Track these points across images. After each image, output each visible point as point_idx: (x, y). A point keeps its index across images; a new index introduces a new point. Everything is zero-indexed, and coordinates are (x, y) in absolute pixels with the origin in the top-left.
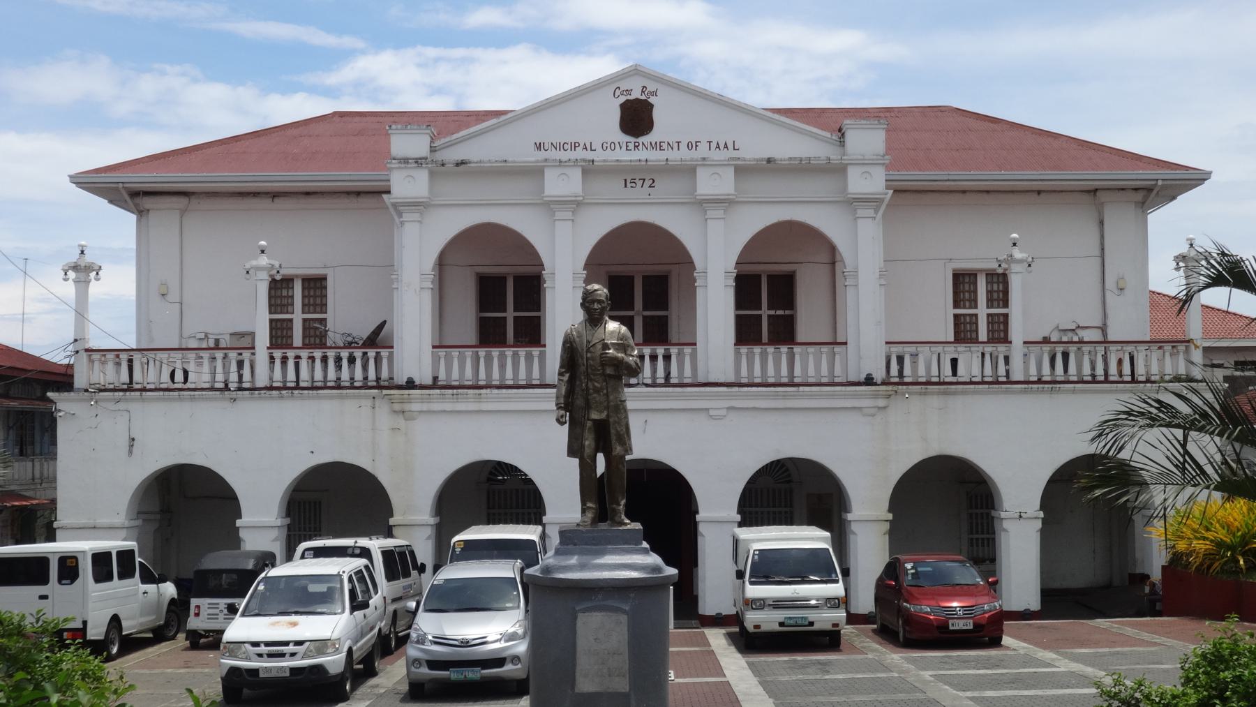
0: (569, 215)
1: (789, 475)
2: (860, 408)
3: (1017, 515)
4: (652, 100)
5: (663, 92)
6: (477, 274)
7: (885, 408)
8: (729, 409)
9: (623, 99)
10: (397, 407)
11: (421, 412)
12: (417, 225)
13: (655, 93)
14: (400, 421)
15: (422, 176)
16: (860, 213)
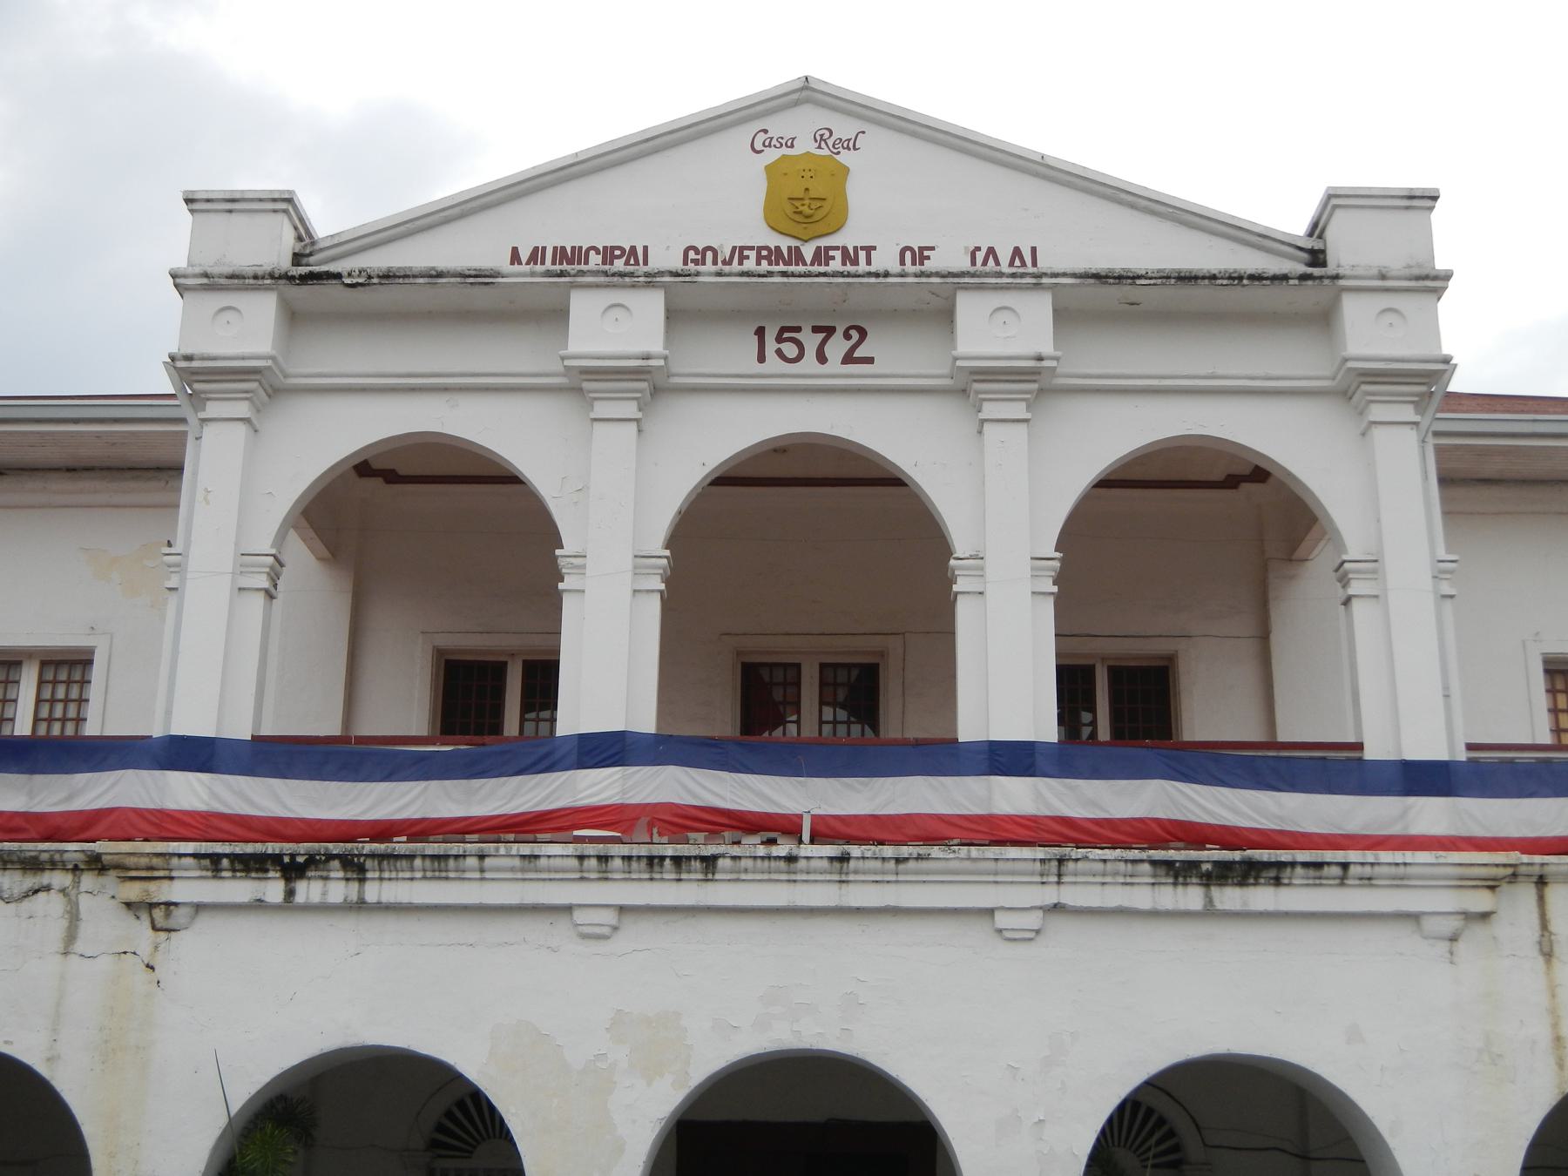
0: (630, 409)
1: (1176, 1148)
2: (1414, 917)
4: (845, 158)
5: (876, 141)
6: (439, 653)
7: (1485, 916)
8: (1057, 908)
9: (772, 155)
10: (133, 891)
11: (199, 908)
12: (241, 429)
13: (851, 145)
14: (140, 933)
15: (263, 309)
16: (1378, 412)
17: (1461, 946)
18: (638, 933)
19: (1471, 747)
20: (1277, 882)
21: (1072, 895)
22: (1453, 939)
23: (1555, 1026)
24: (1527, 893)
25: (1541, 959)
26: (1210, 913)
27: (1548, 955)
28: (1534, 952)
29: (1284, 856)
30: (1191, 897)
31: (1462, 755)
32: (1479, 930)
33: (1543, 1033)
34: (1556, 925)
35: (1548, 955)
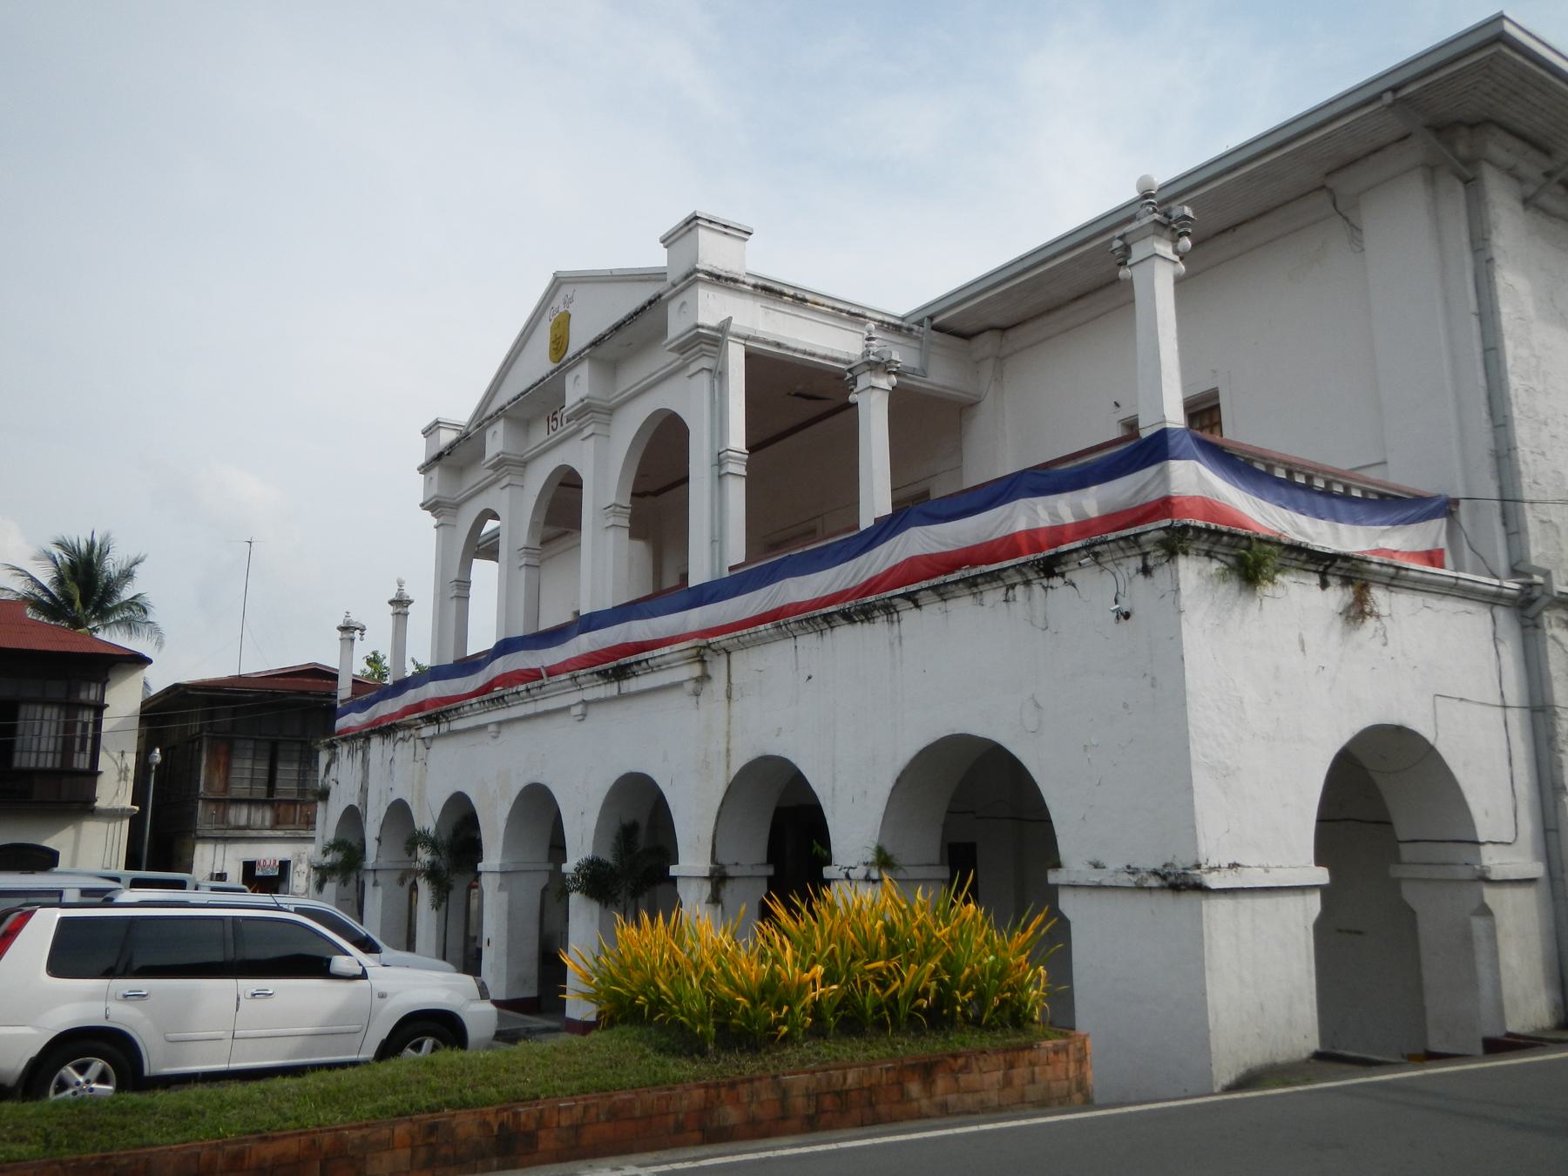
3: (843, 876)
18: (508, 734)
19: (731, 569)
20: (635, 675)
21: (589, 694)
22: (697, 695)
24: (724, 658)
26: (621, 697)
27: (729, 697)
28: (723, 697)
29: (633, 659)
30: (611, 689)
31: (726, 574)
32: (707, 687)
33: (723, 747)
34: (733, 680)
35: (729, 697)
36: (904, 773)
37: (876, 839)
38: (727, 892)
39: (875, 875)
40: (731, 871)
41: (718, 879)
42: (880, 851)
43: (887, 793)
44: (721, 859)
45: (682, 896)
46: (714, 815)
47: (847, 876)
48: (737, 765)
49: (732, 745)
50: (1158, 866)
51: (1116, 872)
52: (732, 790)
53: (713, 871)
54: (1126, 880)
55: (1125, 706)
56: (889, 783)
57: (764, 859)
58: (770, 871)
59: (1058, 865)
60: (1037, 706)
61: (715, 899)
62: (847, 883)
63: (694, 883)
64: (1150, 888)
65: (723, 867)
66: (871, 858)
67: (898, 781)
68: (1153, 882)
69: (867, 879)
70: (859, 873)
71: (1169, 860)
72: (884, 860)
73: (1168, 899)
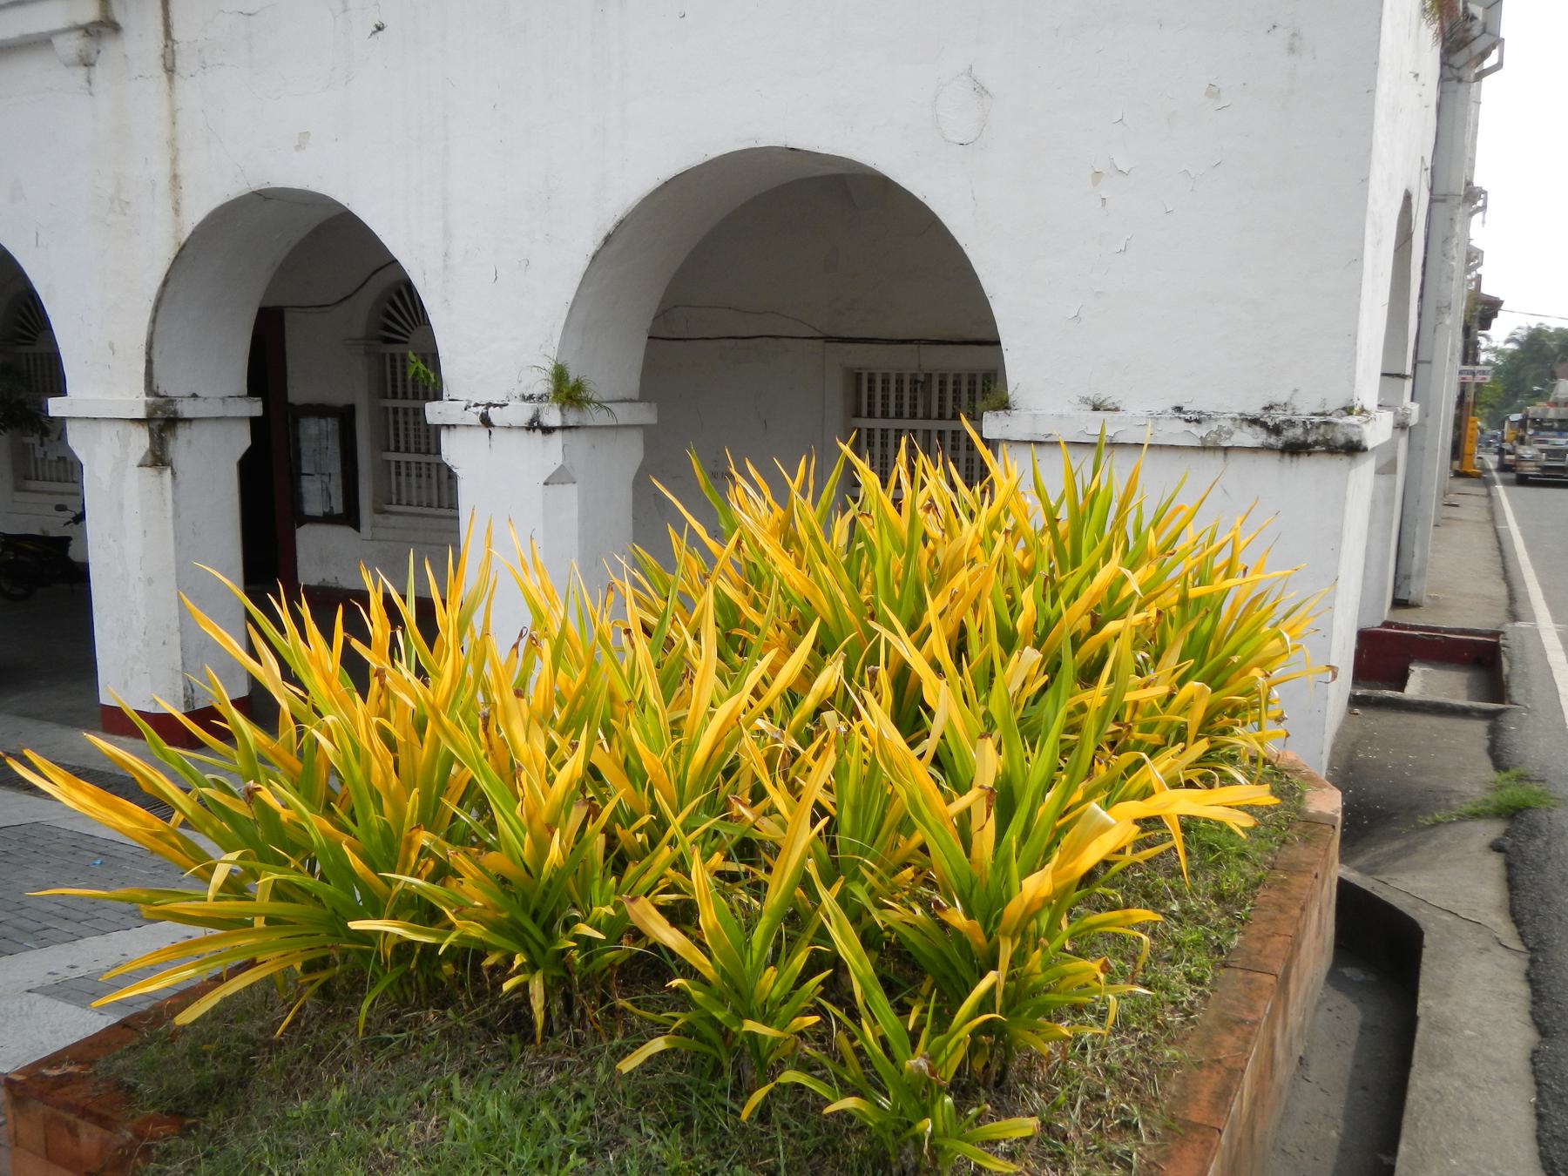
3: (476, 420)
17: (98, 72)
22: (87, 63)
23: (174, 161)
25: (164, 77)
27: (170, 70)
28: (159, 71)
32: (111, 49)
33: (161, 171)
34: (176, 35)
35: (170, 70)
36: (621, 224)
37: (553, 352)
38: (182, 445)
39: (552, 417)
40: (186, 409)
41: (163, 423)
42: (560, 375)
43: (582, 264)
44: (166, 387)
45: (81, 455)
46: (148, 305)
47: (486, 421)
48: (196, 212)
49: (183, 168)
50: (1254, 410)
51: (1155, 417)
52: (185, 257)
53: (152, 409)
54: (1176, 432)
55: (1213, 92)
56: (589, 243)
57: (242, 387)
58: (256, 408)
59: (1004, 405)
60: (980, 90)
61: (158, 459)
62: (484, 432)
63: (107, 431)
64: (1226, 449)
65: (171, 401)
66: (541, 384)
67: (608, 239)
68: (1249, 437)
69: (534, 425)
70: (523, 413)
71: (1281, 398)
72: (568, 391)
73: (1271, 469)
